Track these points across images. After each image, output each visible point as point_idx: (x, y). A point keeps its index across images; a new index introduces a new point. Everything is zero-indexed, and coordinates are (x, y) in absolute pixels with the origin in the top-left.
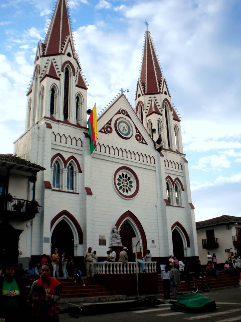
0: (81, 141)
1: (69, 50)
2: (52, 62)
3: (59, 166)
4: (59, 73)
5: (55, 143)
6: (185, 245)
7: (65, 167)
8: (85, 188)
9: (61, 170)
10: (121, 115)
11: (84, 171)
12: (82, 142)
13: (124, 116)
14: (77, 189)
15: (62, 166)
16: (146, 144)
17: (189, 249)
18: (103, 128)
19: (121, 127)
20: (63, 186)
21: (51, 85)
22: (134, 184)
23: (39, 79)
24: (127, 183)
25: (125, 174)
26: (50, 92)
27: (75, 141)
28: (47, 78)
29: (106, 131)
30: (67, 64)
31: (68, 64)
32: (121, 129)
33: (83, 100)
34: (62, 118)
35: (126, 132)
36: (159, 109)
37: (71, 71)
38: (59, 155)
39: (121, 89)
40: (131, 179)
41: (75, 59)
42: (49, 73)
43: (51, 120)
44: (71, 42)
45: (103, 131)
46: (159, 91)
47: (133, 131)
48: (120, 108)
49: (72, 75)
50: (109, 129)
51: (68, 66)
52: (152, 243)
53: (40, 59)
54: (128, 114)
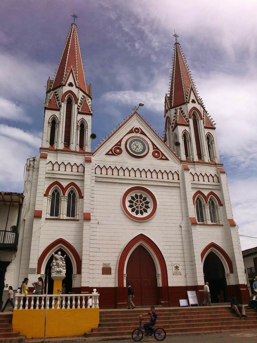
0: (217, 176)
1: (192, 97)
10: (134, 134)
13: (138, 135)
16: (167, 159)
22: (151, 205)
23: (171, 129)
29: (114, 153)
32: (134, 148)
34: (196, 159)
41: (199, 104)
52: (175, 270)
53: (169, 111)
54: (143, 131)
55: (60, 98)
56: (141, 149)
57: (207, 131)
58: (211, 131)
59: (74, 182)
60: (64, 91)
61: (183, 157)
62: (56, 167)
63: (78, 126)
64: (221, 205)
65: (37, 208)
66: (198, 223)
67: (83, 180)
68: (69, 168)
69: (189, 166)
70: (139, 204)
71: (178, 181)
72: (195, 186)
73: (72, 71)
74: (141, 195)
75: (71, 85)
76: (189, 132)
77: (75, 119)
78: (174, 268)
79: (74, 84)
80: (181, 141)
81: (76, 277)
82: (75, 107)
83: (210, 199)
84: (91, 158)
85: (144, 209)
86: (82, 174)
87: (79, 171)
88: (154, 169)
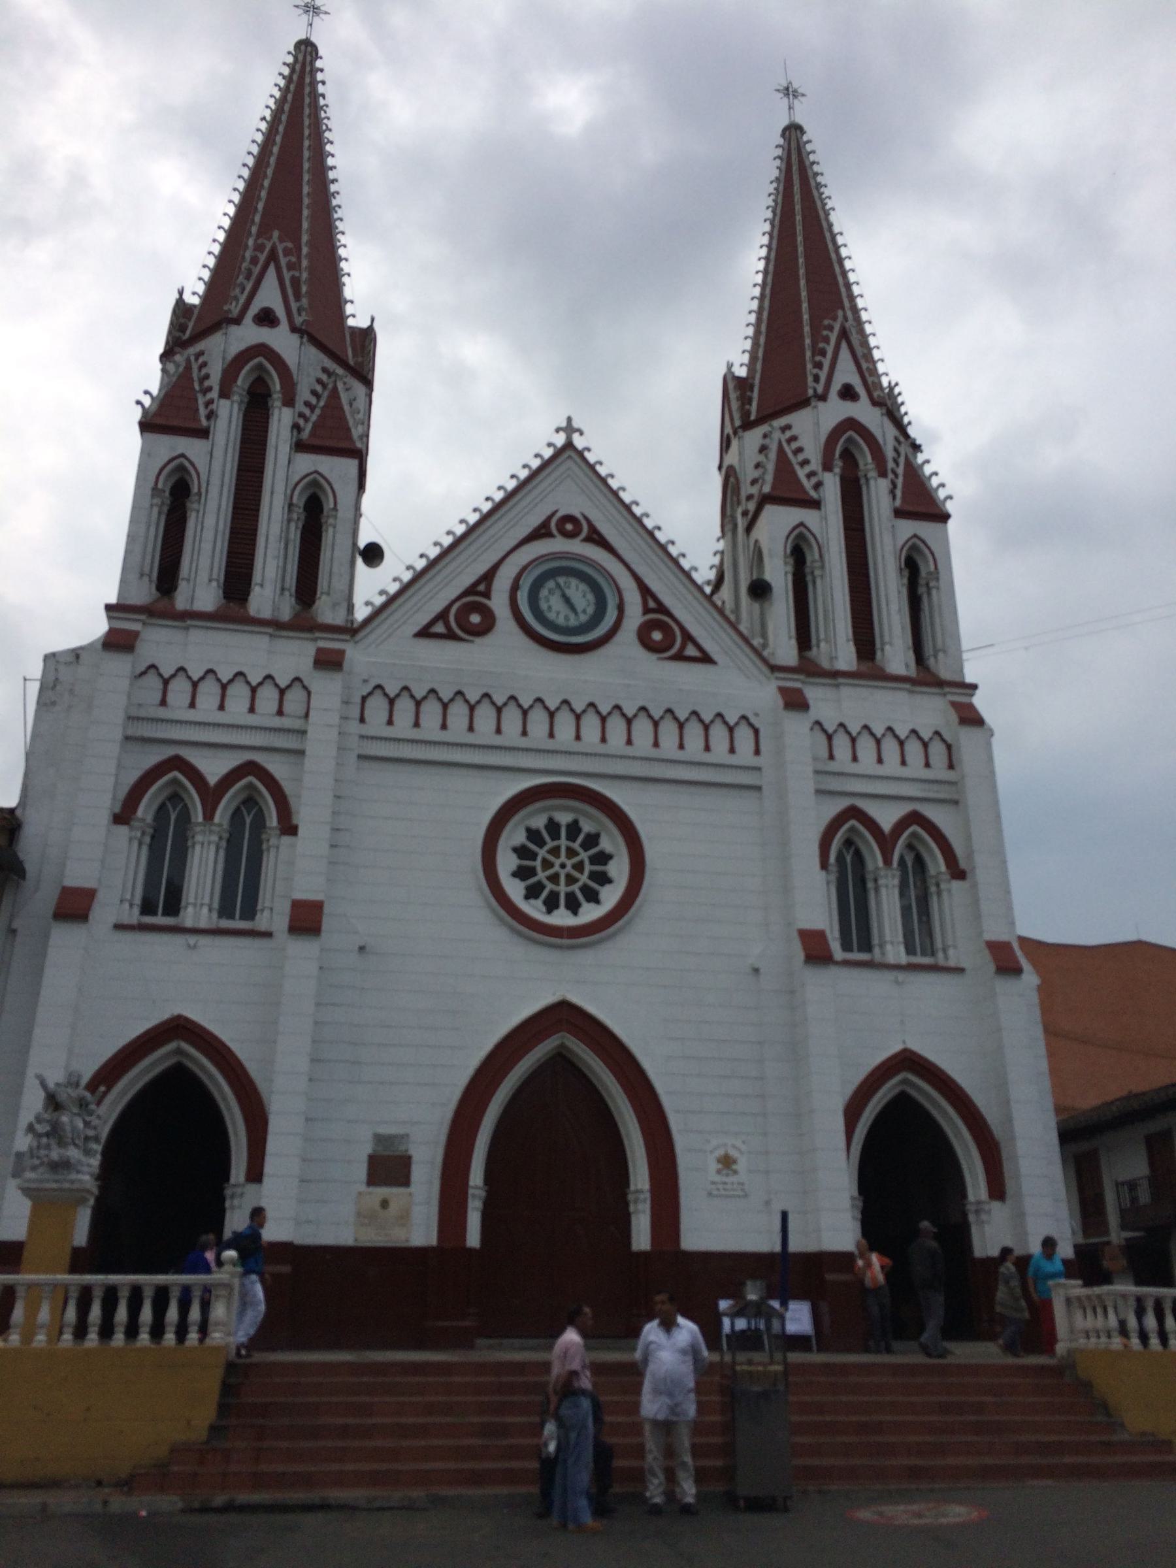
1: (846, 373)
2: (780, 443)
3: (858, 855)
4: (814, 480)
5: (833, 766)
6: (976, 1186)
7: (887, 861)
8: (983, 945)
9: (869, 877)
10: (558, 544)
11: (974, 868)
12: (949, 747)
13: (577, 547)
14: (951, 952)
15: (874, 858)
16: (706, 659)
17: (998, 1212)
18: (443, 616)
19: (548, 600)
20: (885, 942)
21: (157, 471)
23: (741, 523)
24: (579, 867)
25: (539, 822)
26: (786, 563)
27: (871, 744)
28: (770, 510)
30: (845, 432)
31: (850, 433)
32: (550, 608)
33: (821, 556)
35: (572, 616)
36: (804, 480)
37: (866, 460)
38: (177, 763)
39: (564, 424)
40: (605, 844)
41: (875, 403)
42: (773, 487)
43: (802, 677)
44: (855, 339)
45: (439, 628)
46: (810, 392)
47: (621, 608)
48: (549, 513)
49: (872, 474)
50: (475, 619)
51: (850, 440)
55: (215, 381)
56: (584, 611)
57: (908, 528)
58: (924, 529)
59: (259, 758)
60: (235, 349)
61: (785, 650)
62: (179, 690)
63: (291, 505)
64: (958, 873)
65: (78, 876)
66: (838, 954)
67: (301, 753)
68: (238, 696)
69: (816, 694)
70: (563, 866)
71: (752, 760)
72: (835, 784)
73: (273, 257)
74: (576, 822)
75: (266, 318)
76: (818, 536)
77: (281, 474)
78: (713, 1166)
79: (280, 312)
80: (778, 574)
81: (242, 1195)
82: (281, 422)
83: (910, 847)
84: (342, 653)
85: (585, 889)
86: (297, 724)
87: (287, 708)
88: (485, 691)
